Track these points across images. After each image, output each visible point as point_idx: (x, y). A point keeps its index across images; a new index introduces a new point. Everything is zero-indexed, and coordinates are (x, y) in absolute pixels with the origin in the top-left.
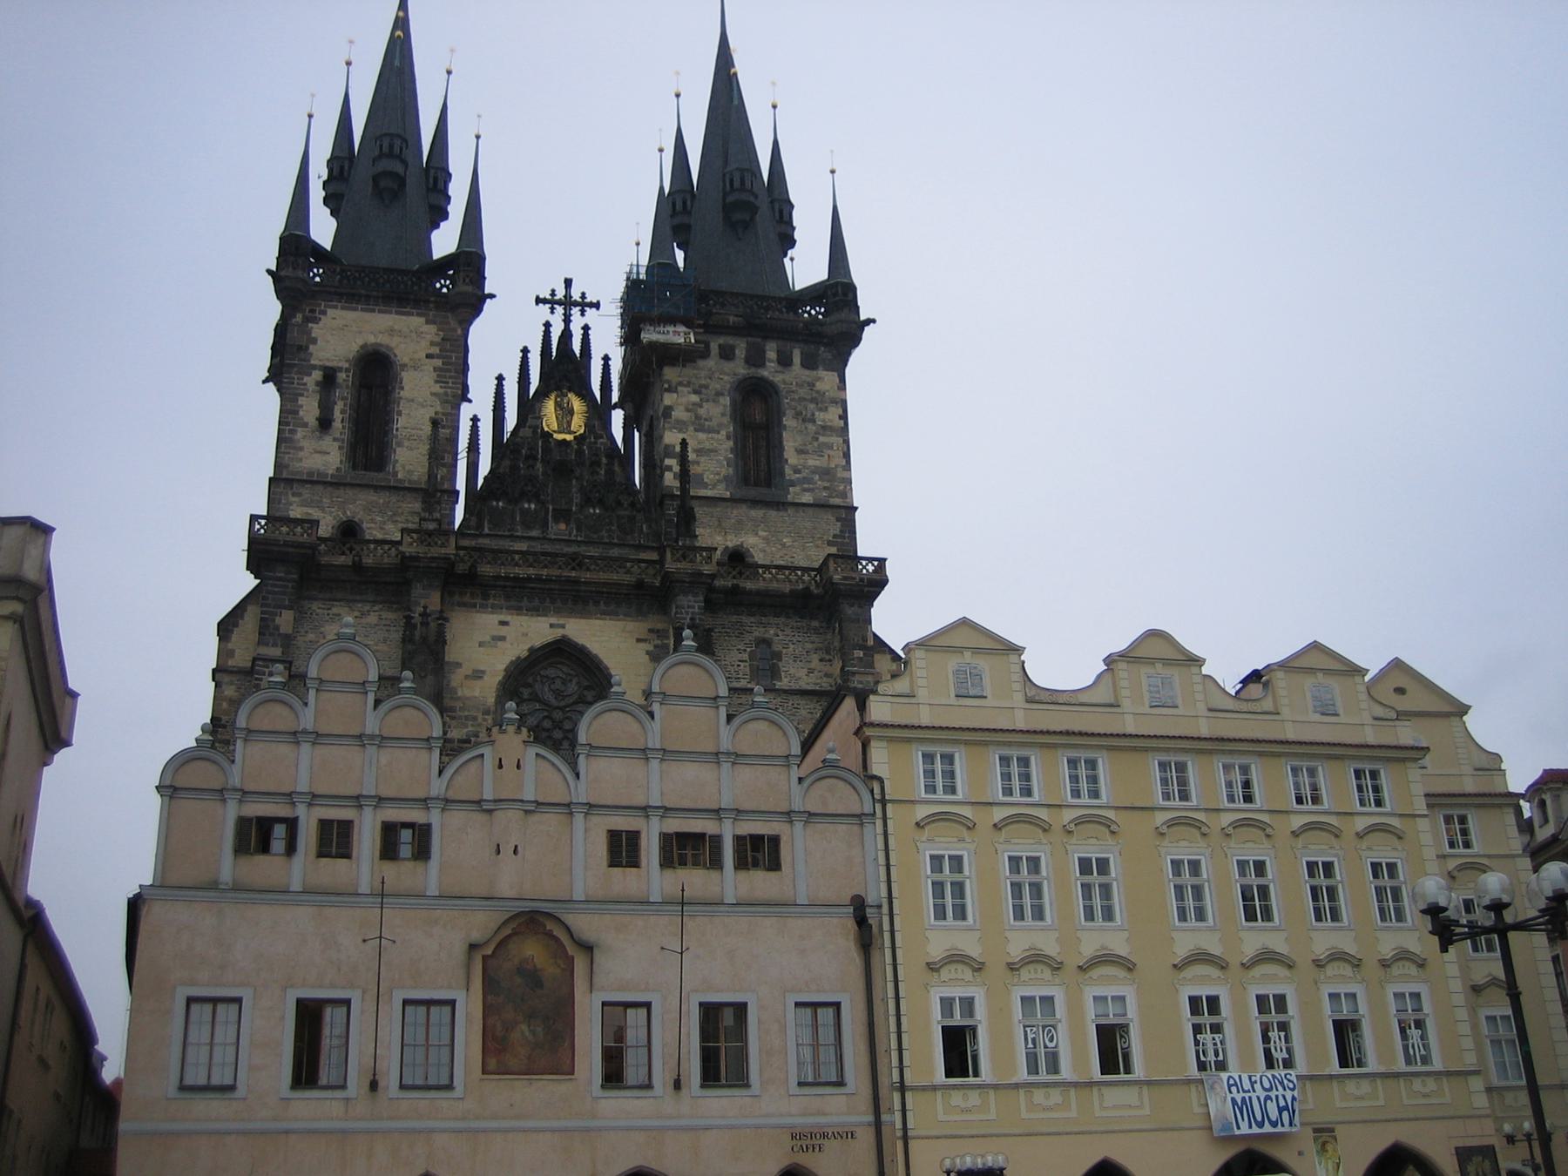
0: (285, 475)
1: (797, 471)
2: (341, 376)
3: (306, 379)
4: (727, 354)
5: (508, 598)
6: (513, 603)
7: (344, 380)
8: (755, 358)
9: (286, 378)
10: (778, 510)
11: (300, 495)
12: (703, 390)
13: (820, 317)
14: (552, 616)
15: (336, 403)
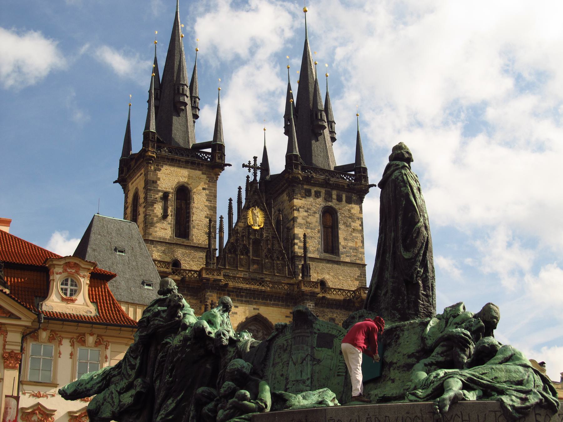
0: (150, 238)
1: (344, 248)
2: (171, 195)
3: (157, 196)
4: (317, 195)
5: (237, 296)
6: (240, 298)
7: (171, 197)
8: (328, 197)
9: (149, 195)
10: (337, 264)
11: (156, 247)
12: (309, 211)
13: (353, 181)
14: (254, 305)
15: (168, 208)
